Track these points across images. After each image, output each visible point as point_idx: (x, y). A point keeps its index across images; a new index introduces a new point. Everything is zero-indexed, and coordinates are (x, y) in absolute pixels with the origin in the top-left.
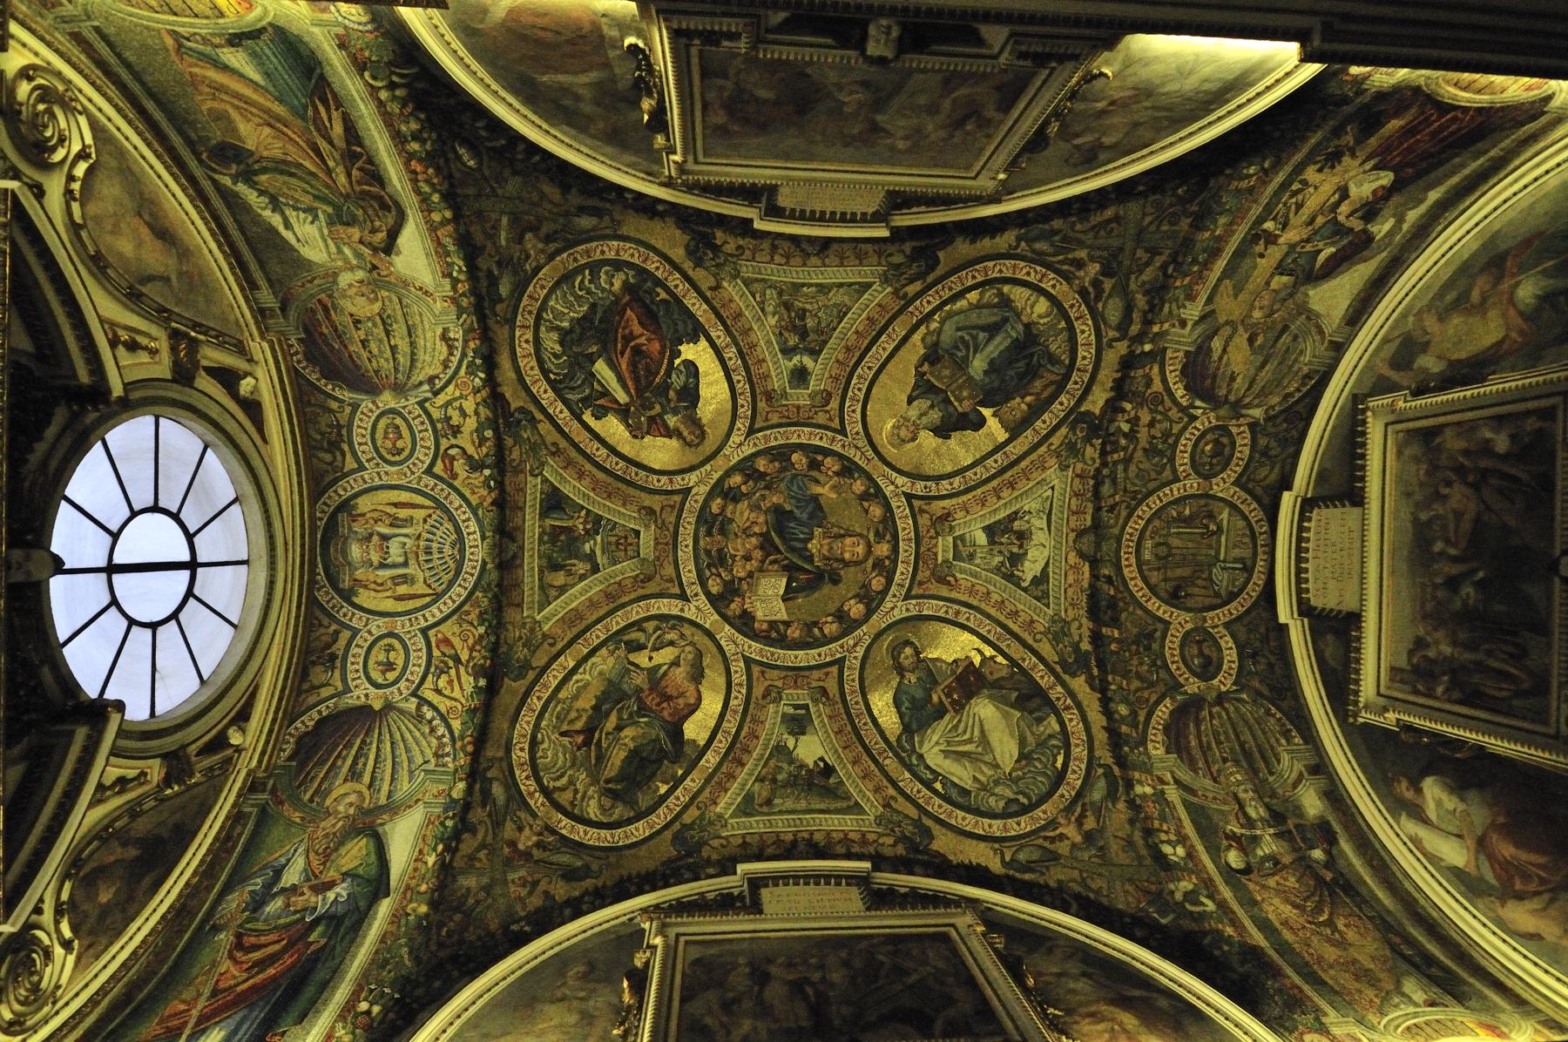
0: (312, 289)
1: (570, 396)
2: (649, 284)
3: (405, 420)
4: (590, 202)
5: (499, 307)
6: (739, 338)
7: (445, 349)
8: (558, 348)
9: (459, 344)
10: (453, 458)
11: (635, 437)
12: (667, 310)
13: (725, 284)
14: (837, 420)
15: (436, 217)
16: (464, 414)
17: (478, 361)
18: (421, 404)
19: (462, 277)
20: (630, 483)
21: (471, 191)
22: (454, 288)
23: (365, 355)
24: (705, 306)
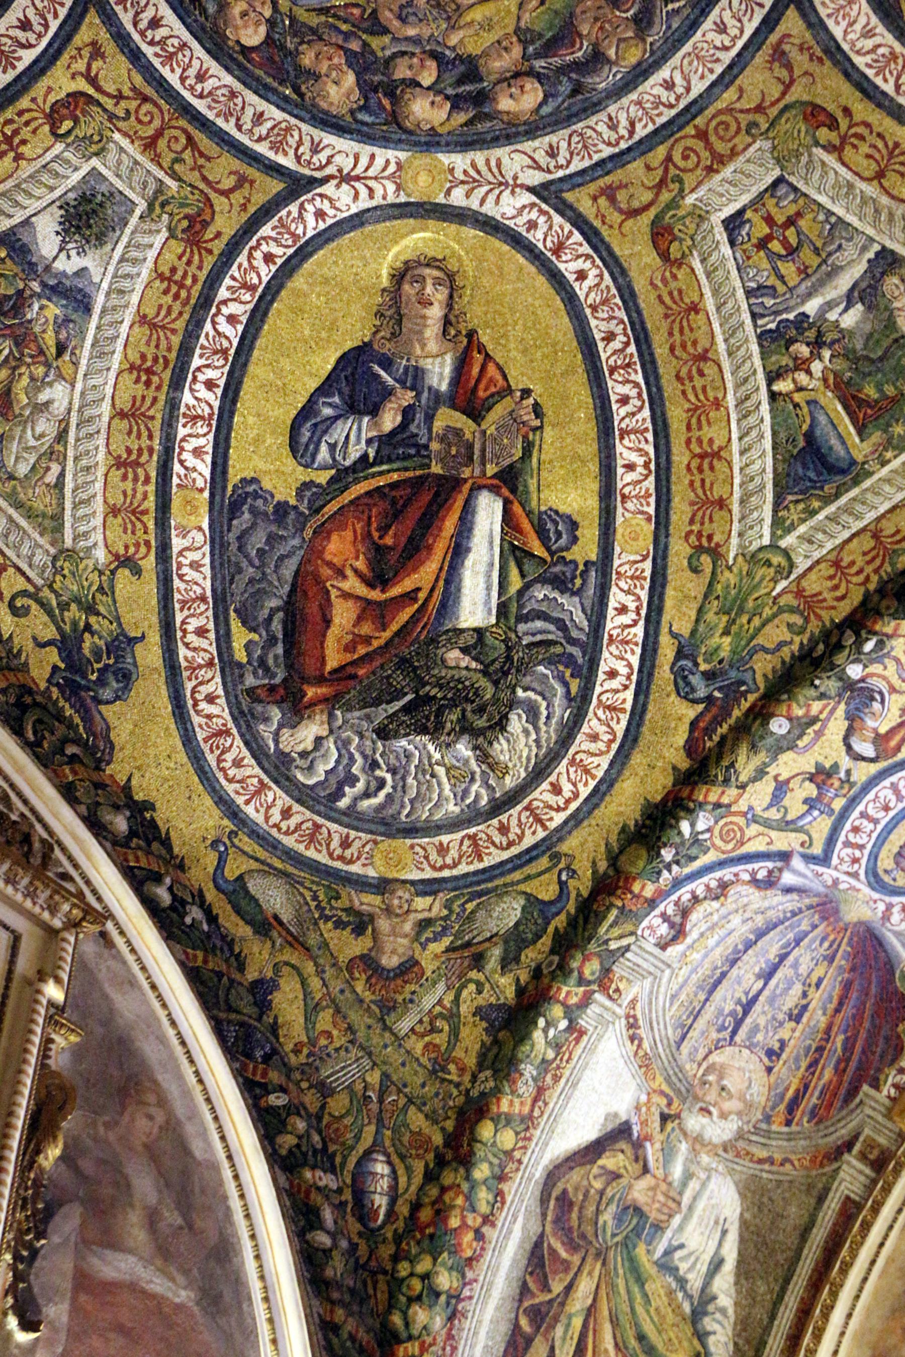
0: (778, 1149)
1: (580, 618)
2: (250, 681)
3: (874, 857)
4: (241, 930)
5: (546, 891)
6: (158, 412)
7: (694, 917)
8: (516, 723)
9: (668, 906)
10: (880, 740)
11: (537, 410)
12: (259, 595)
13: (101, 555)
14: (83, 36)
15: (507, 1139)
16: (781, 787)
17: (667, 854)
18: (824, 860)
19: (557, 1011)
20: (642, 338)
21: (416, 1120)
22: (586, 1001)
23: (816, 998)
24: (177, 543)
